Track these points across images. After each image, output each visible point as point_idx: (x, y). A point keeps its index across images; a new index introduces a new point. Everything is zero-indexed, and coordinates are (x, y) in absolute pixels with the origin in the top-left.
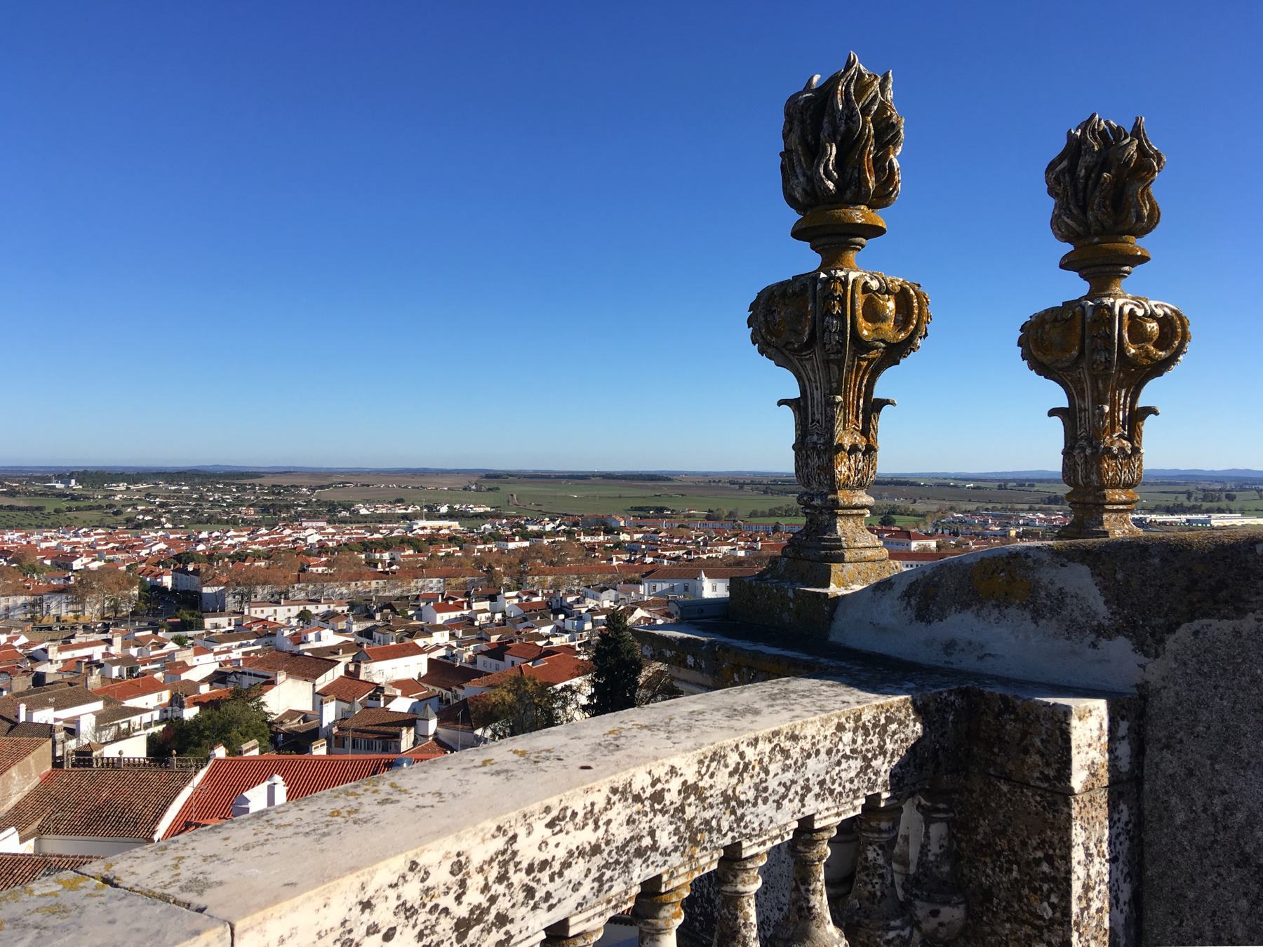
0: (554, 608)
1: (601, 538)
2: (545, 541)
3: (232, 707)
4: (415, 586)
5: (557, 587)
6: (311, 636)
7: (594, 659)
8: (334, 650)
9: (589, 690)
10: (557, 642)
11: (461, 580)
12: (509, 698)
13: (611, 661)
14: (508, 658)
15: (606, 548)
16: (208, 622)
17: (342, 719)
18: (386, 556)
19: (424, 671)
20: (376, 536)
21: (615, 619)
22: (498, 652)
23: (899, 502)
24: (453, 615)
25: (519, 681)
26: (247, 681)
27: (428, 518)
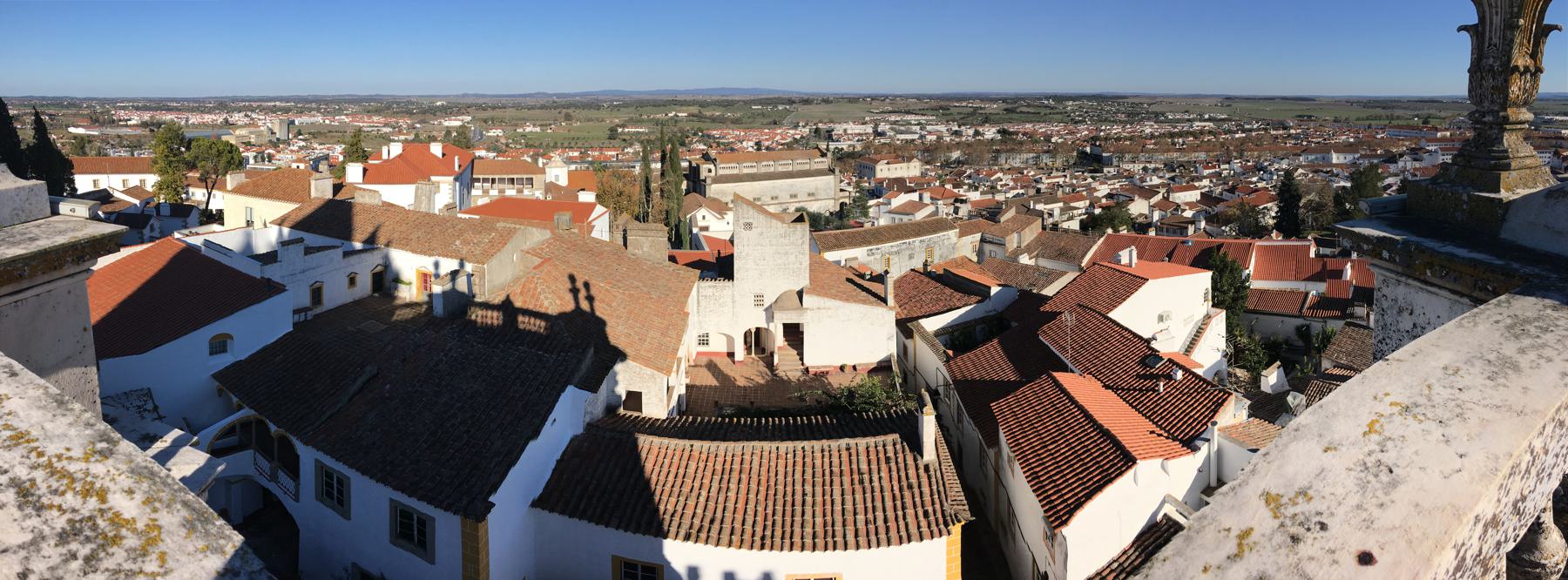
0: (1259, 168)
1: (1281, 132)
2: (1254, 134)
3: (1116, 210)
4: (1193, 156)
5: (1259, 157)
6: (1148, 179)
7: (1278, 194)
8: (1158, 186)
9: (1276, 209)
10: (1260, 185)
11: (1215, 153)
12: (1238, 212)
13: (1287, 195)
14: (1237, 193)
15: (1284, 138)
16: (1105, 170)
17: (1162, 219)
18: (1181, 140)
19: (1199, 198)
20: (1176, 130)
21: (1289, 174)
22: (1232, 190)
23: (1432, 112)
24: (1211, 171)
25: (1242, 204)
26: (1122, 198)
27: (1200, 121)
